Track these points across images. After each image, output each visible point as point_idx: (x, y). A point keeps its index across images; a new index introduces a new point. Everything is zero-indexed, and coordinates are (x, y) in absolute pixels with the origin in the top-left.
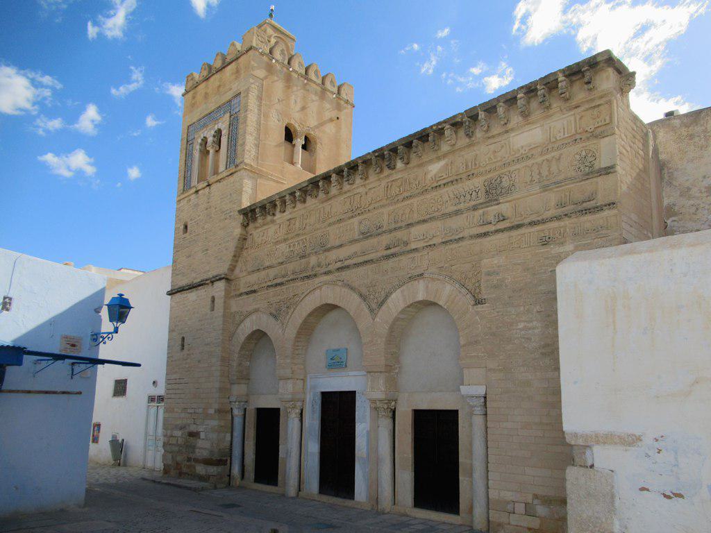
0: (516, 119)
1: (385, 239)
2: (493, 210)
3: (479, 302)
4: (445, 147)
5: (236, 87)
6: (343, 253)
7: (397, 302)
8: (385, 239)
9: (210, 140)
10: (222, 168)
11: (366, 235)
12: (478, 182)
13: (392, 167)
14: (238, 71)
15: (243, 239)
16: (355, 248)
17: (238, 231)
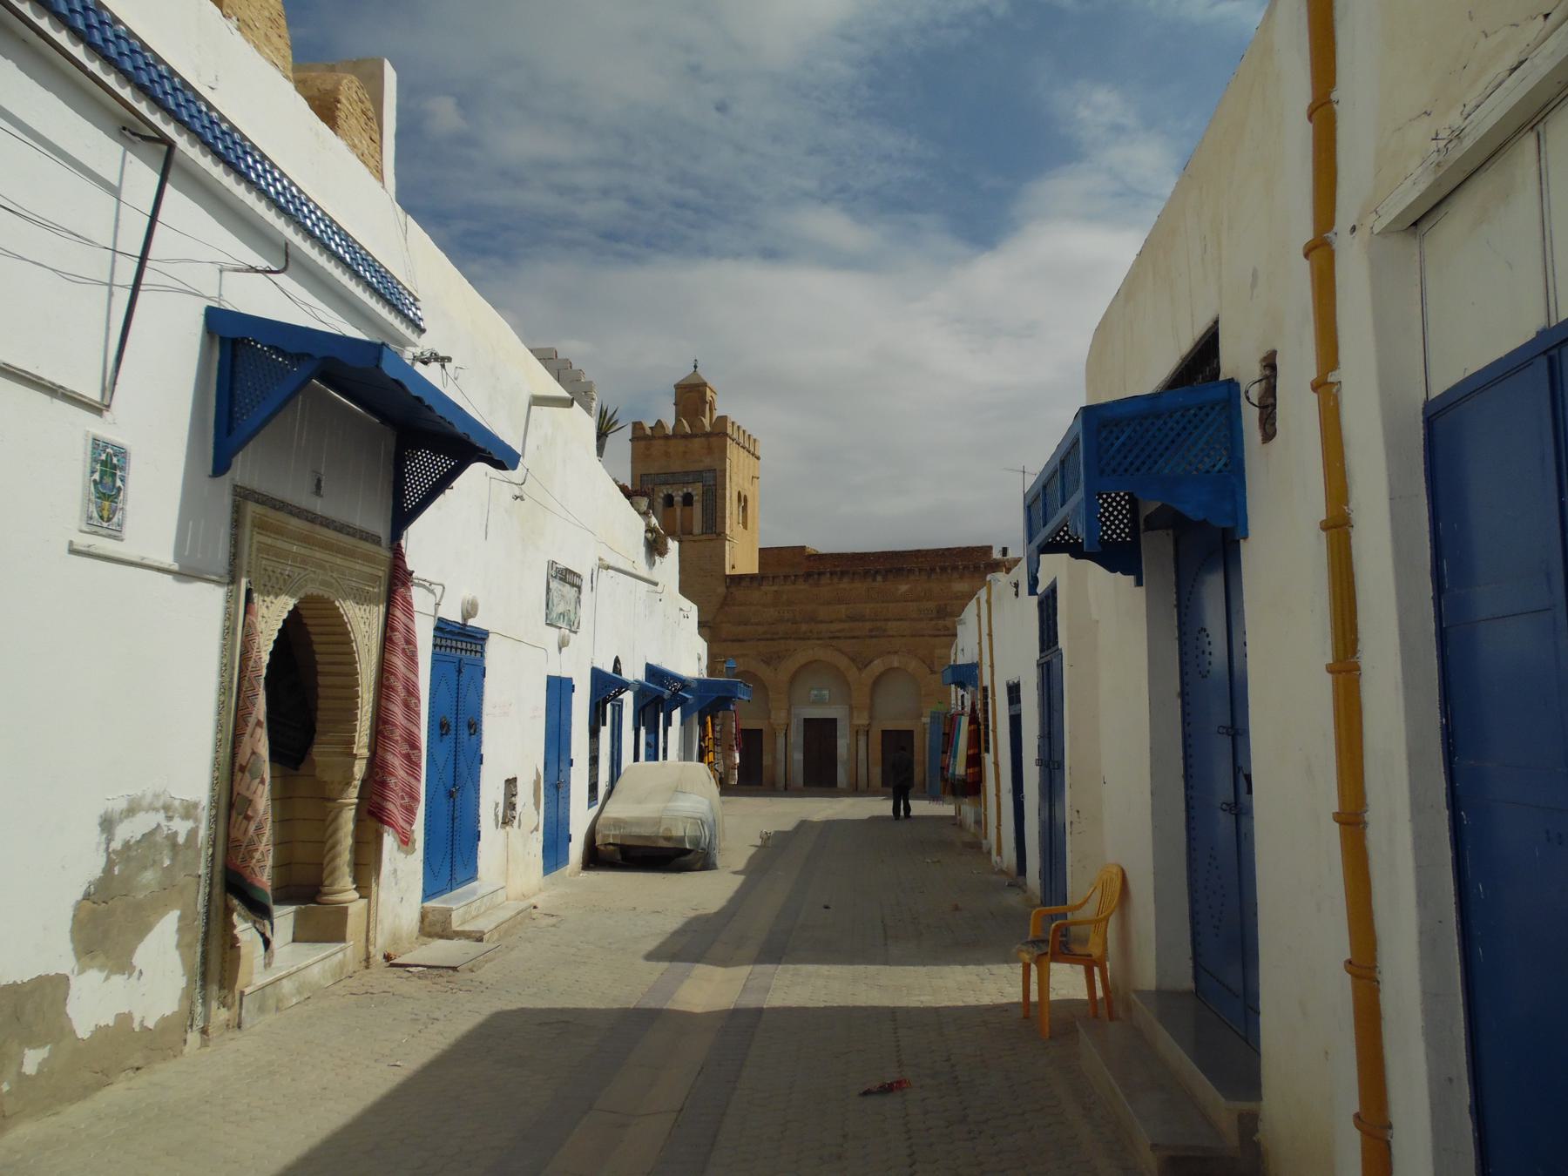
0: (956, 575)
1: (868, 625)
2: (941, 623)
3: (933, 672)
4: (912, 578)
5: (707, 462)
6: (835, 627)
7: (877, 666)
8: (868, 625)
9: (678, 499)
10: (697, 529)
11: (852, 619)
12: (931, 605)
13: (874, 580)
14: (710, 450)
15: (725, 598)
16: (846, 625)
17: (722, 590)
